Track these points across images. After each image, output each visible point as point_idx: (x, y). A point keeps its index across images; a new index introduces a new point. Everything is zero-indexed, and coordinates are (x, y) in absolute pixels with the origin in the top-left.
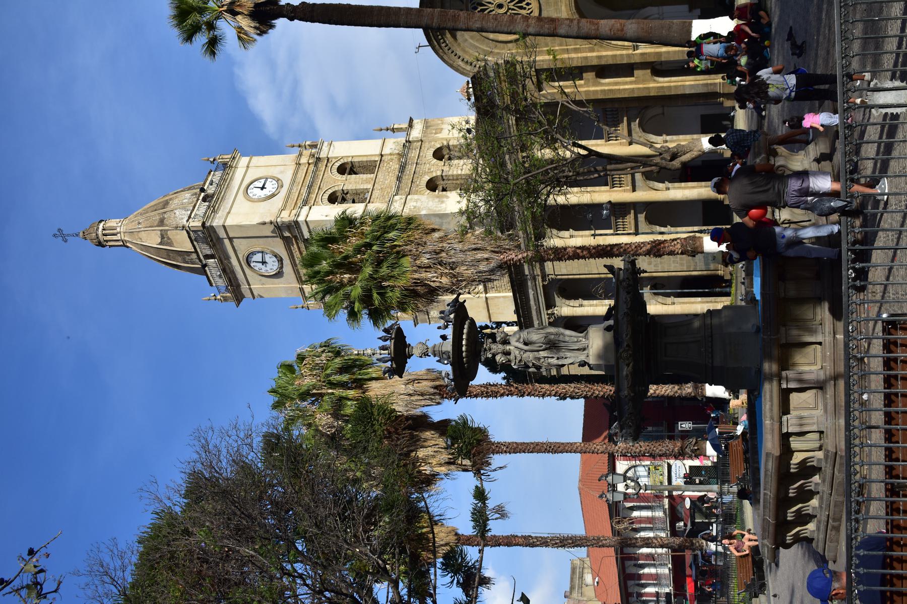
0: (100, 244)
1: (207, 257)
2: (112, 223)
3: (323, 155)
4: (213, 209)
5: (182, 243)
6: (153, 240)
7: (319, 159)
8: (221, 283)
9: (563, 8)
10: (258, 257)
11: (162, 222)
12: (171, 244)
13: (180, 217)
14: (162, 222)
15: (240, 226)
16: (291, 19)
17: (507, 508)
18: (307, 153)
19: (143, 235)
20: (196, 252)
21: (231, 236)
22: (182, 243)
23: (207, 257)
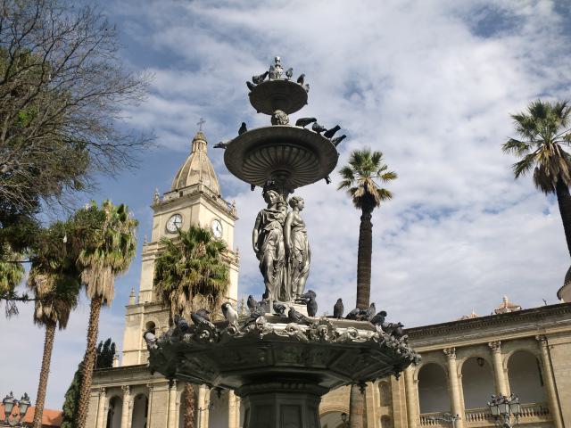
0: (195, 140)
1: (181, 194)
2: (205, 148)
3: (231, 265)
4: (208, 200)
5: (191, 181)
6: (194, 166)
7: (229, 263)
8: (166, 198)
9: (329, 404)
10: (178, 220)
11: (204, 172)
12: (191, 175)
13: (206, 182)
14: (204, 172)
15: (198, 212)
16: (361, 218)
17: (14, 317)
18: (232, 256)
19: (198, 162)
20: (185, 188)
21: (194, 207)
22: (191, 181)
23: (181, 194)
